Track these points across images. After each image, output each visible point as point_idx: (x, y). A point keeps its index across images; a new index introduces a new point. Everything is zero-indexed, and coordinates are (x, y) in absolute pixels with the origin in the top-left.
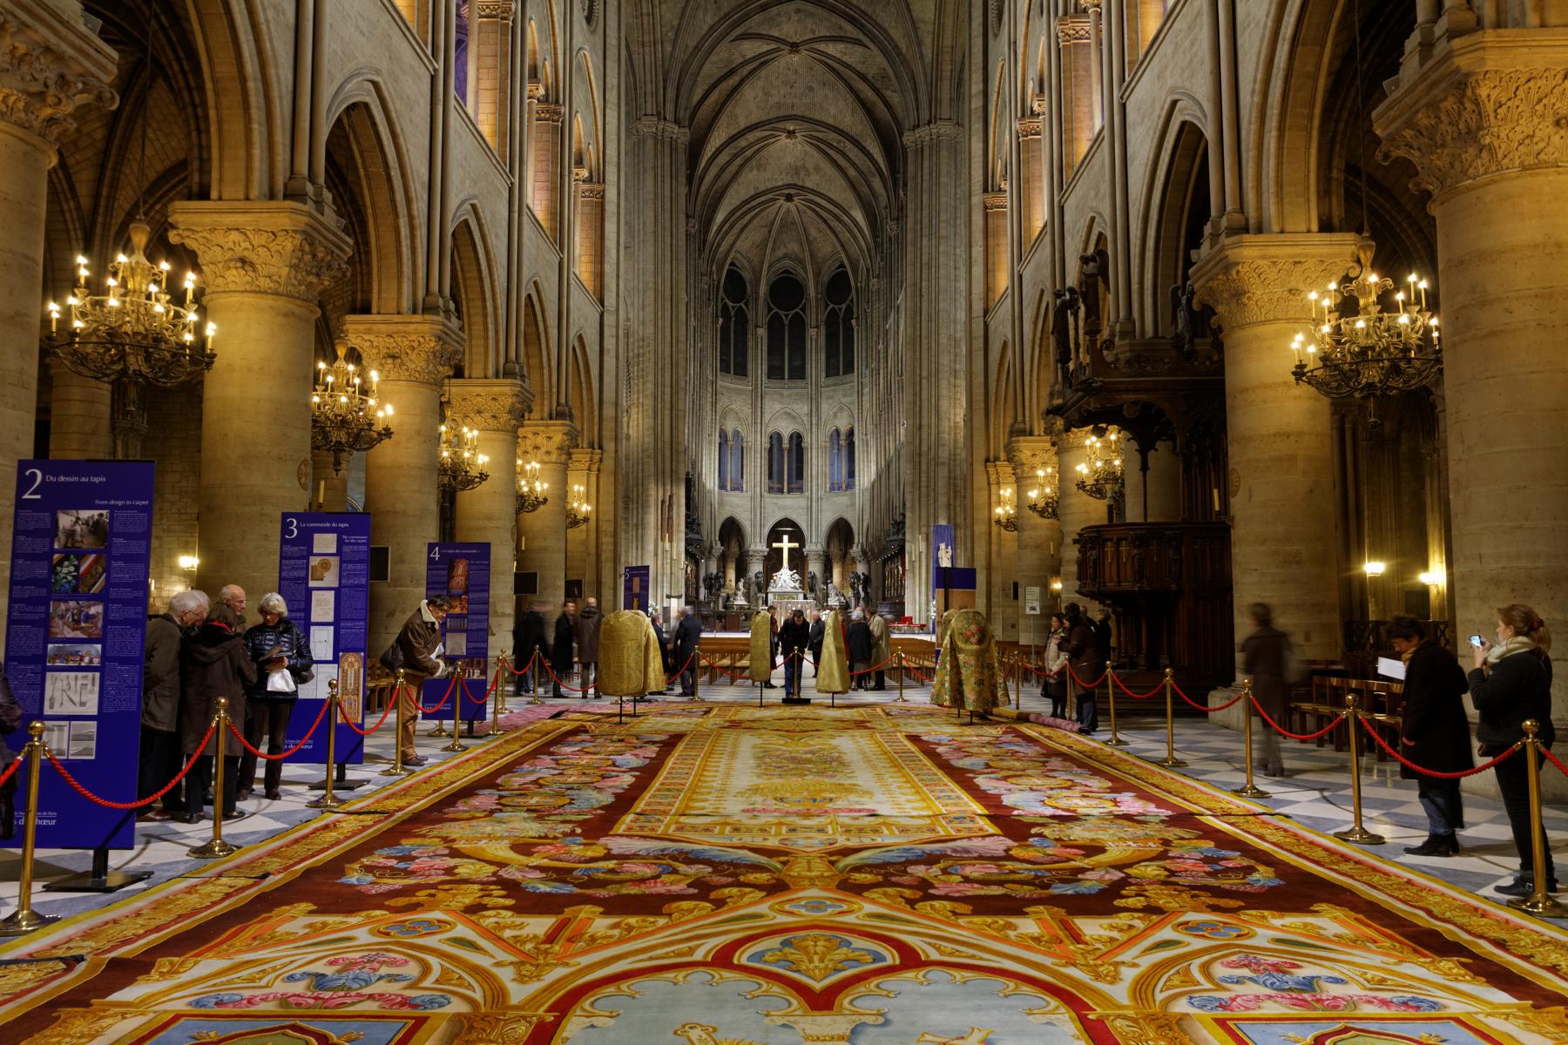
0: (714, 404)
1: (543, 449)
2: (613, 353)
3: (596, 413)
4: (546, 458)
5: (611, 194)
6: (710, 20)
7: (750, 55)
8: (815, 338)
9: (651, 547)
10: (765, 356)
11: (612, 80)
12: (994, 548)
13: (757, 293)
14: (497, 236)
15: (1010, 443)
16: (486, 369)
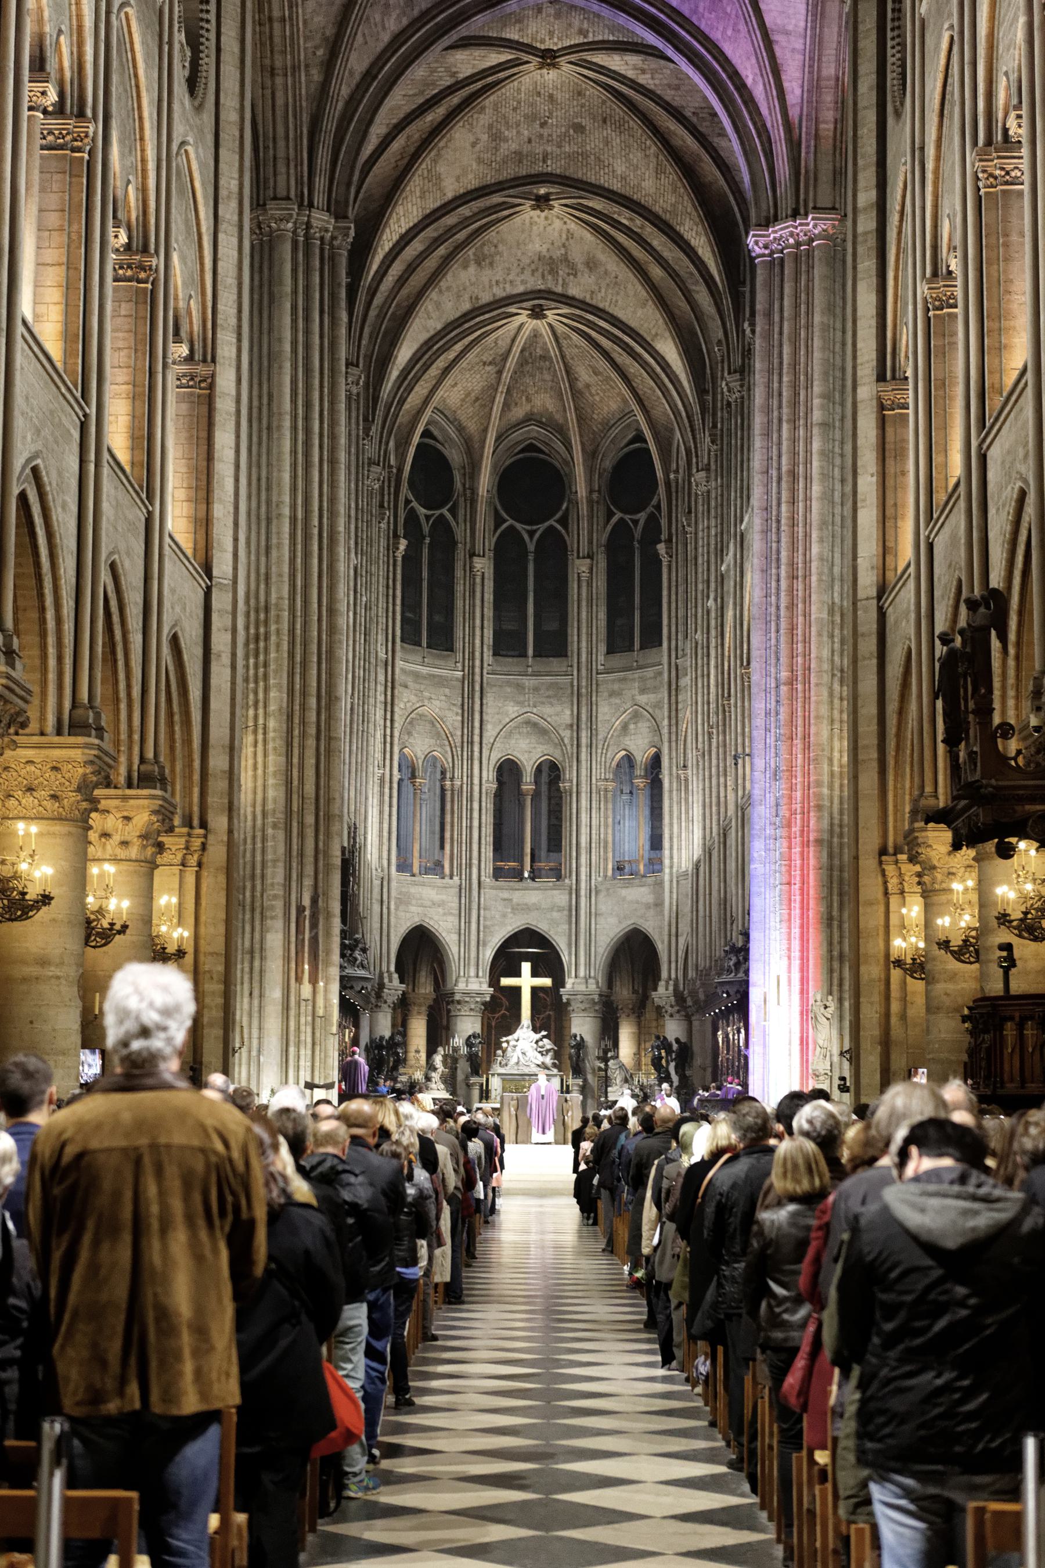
0: (390, 705)
1: (117, 838)
2: (226, 659)
3: (197, 764)
4: (122, 853)
5: (226, 381)
6: (393, 24)
7: (466, 71)
8: (587, 578)
9: (275, 994)
10: (489, 612)
11: (230, 183)
12: (895, 1007)
13: (474, 491)
14: (64, 506)
15: (912, 831)
16: (43, 719)
